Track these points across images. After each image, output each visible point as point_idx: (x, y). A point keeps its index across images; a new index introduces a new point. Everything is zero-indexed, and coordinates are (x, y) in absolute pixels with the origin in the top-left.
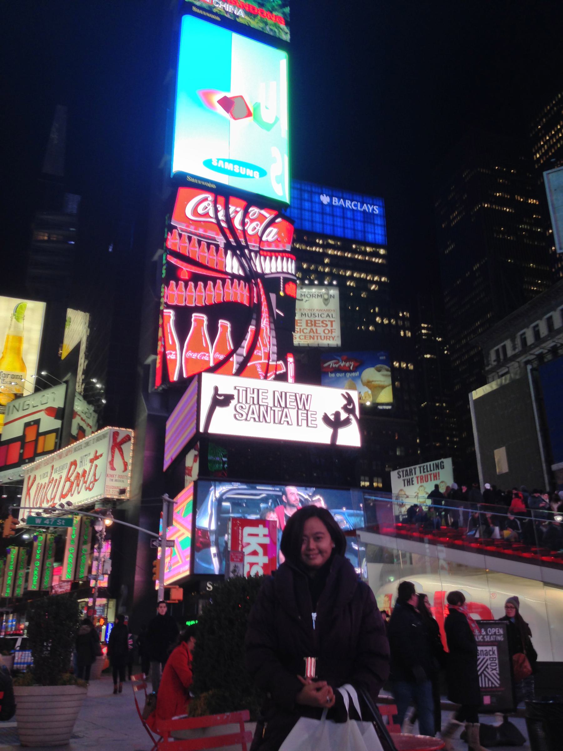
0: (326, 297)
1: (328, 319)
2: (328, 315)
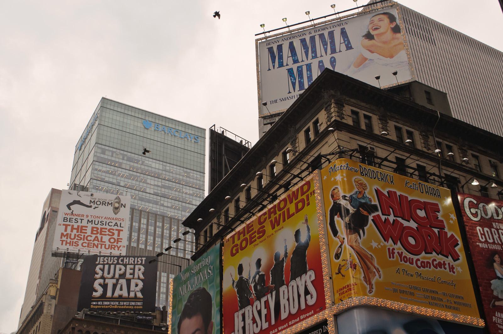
0: (117, 205)
1: (116, 227)
2: (116, 224)
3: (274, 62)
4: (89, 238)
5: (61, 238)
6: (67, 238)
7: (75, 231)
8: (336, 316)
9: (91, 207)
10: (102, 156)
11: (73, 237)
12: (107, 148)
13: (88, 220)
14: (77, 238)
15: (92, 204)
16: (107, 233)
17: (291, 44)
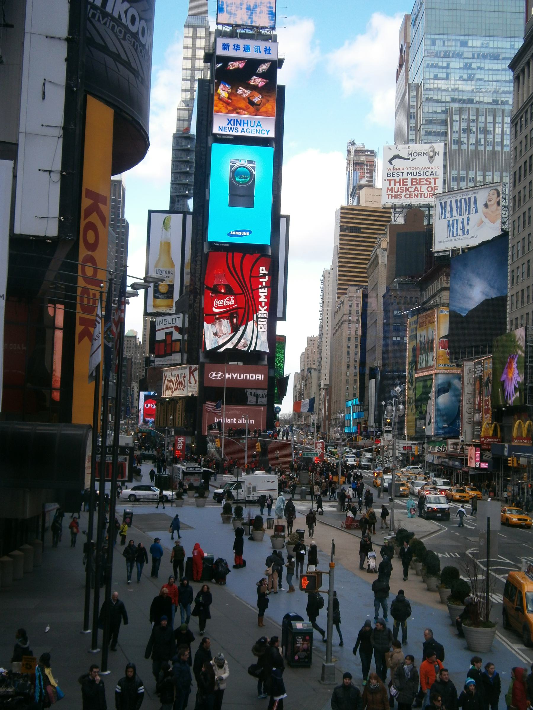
0: (431, 154)
1: (432, 176)
2: (432, 173)
3: (442, 214)
4: (410, 190)
5: (387, 192)
6: (392, 192)
7: (398, 184)
8: (436, 374)
9: (409, 159)
10: (433, 48)
11: (396, 190)
12: (437, 37)
13: (408, 173)
14: (400, 190)
15: (410, 156)
16: (425, 182)
17: (451, 202)
